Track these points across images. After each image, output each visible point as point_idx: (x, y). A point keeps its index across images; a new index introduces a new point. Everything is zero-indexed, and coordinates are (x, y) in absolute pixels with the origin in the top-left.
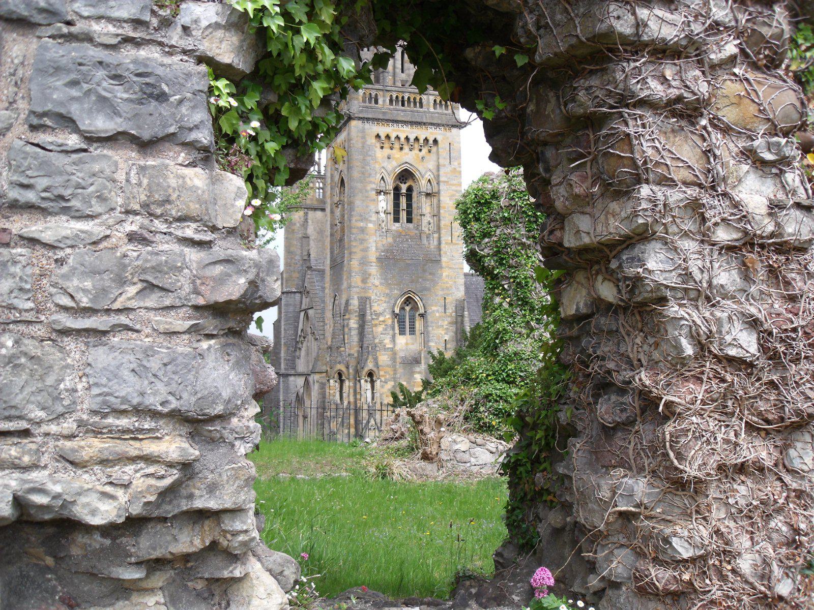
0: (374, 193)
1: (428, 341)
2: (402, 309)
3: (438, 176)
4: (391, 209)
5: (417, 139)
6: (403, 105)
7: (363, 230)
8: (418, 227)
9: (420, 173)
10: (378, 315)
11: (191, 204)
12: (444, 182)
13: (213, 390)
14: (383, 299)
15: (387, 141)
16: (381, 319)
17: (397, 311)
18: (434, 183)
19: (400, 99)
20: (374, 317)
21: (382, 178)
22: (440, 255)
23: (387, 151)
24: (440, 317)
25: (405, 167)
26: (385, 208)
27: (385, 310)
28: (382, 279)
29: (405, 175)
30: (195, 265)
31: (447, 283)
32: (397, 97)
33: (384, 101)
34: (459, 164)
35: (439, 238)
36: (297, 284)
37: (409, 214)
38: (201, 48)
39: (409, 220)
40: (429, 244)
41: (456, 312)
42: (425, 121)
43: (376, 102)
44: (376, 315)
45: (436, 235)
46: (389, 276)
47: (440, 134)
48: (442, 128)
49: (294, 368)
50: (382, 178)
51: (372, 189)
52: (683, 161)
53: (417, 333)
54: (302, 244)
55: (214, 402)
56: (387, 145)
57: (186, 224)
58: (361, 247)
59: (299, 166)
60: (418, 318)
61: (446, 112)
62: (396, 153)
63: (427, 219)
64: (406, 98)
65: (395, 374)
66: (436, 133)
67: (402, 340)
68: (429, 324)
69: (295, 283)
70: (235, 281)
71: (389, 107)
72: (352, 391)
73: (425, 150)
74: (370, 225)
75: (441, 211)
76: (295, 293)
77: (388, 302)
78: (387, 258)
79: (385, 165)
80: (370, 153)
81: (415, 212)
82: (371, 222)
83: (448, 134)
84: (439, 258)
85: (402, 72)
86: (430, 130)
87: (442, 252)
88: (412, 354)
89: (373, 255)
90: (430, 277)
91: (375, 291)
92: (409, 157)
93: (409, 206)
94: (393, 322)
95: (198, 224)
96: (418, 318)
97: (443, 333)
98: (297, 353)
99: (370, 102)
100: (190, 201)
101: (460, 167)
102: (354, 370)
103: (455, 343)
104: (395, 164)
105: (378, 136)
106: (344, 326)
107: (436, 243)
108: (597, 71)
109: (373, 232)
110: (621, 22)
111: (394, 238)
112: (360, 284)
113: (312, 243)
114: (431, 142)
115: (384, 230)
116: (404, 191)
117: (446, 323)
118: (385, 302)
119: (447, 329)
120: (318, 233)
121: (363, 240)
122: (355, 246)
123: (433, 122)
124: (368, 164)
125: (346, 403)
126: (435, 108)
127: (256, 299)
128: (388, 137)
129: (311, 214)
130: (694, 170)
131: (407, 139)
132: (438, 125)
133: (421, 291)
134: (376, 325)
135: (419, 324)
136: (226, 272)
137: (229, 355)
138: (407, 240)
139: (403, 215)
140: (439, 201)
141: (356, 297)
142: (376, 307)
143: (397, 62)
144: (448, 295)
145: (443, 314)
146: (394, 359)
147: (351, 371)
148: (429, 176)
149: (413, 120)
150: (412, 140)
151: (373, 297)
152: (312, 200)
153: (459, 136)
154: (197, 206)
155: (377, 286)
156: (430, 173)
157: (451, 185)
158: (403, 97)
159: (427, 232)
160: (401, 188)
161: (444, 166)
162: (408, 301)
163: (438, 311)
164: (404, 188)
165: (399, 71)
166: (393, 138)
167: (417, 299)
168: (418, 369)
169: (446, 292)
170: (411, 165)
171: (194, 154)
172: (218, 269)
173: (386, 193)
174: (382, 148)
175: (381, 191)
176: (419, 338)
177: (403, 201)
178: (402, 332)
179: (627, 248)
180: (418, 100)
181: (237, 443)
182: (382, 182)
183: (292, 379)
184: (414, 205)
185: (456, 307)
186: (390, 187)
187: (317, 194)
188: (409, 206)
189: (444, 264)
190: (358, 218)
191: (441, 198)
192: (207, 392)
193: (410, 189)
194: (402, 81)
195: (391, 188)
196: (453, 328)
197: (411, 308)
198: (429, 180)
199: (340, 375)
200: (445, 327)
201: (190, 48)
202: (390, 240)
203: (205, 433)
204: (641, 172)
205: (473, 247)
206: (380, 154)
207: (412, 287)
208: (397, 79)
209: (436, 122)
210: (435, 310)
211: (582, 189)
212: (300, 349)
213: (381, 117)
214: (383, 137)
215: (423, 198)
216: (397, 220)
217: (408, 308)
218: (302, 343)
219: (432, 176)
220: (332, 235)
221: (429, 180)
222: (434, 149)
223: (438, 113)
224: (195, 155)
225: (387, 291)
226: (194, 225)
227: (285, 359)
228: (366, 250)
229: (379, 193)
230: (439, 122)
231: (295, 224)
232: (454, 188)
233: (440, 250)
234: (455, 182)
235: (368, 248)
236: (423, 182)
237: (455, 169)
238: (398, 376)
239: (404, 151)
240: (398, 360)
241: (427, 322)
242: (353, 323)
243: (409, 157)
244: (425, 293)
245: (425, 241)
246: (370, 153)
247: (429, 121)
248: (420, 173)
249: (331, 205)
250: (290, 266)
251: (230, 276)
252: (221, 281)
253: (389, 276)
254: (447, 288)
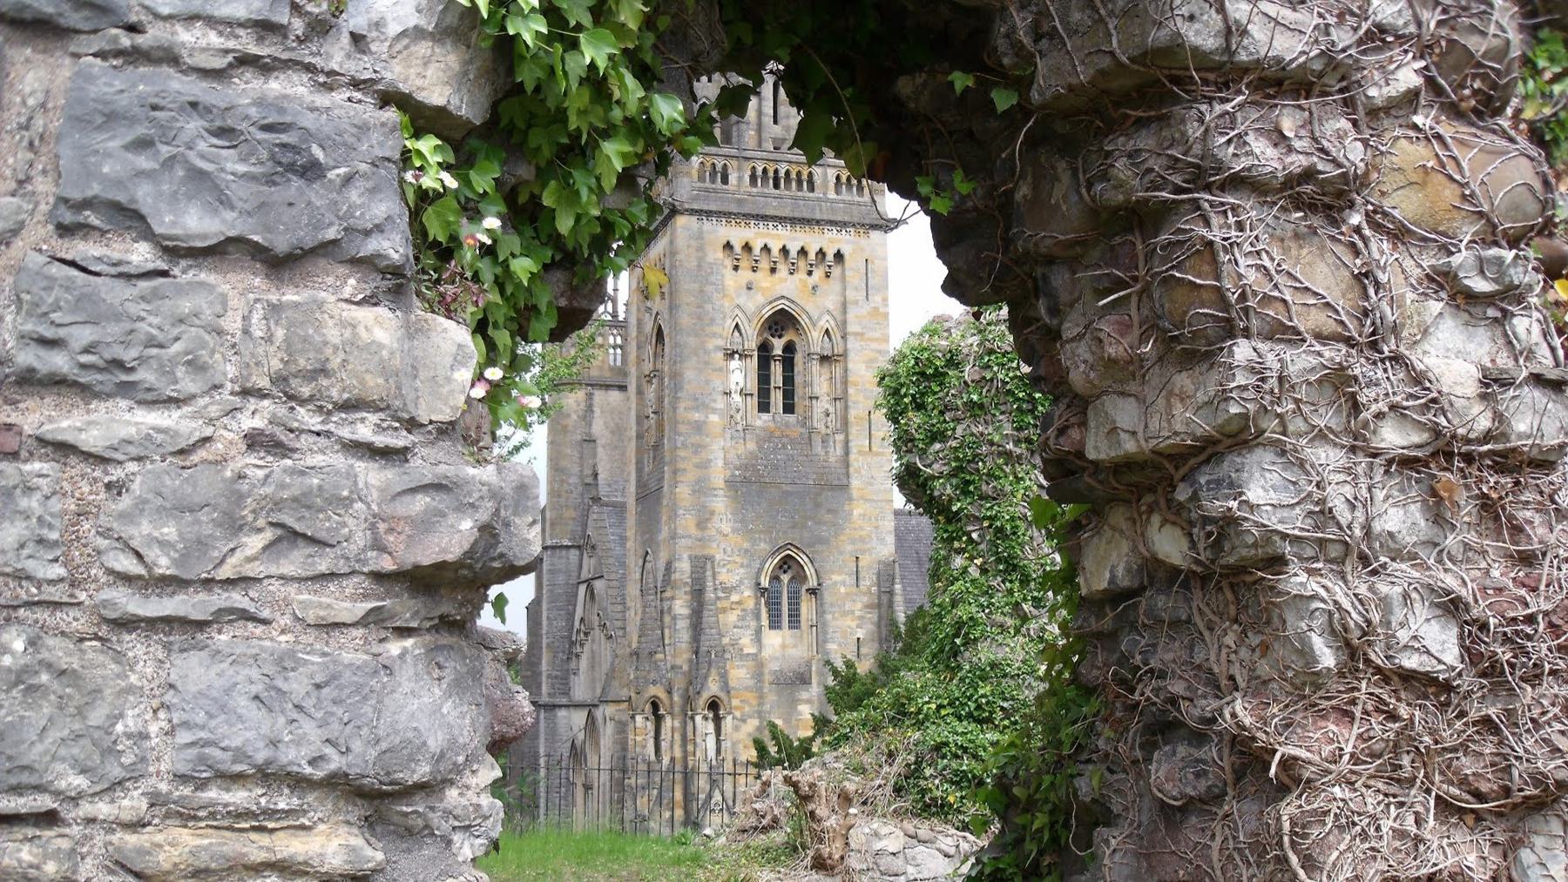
0: (720, 355)
1: (825, 641)
2: (775, 578)
3: (845, 322)
4: (753, 386)
5: (803, 252)
6: (776, 186)
7: (699, 427)
8: (805, 421)
9: (810, 318)
10: (728, 590)
11: (368, 377)
12: (856, 334)
13: (410, 735)
14: (738, 559)
15: (745, 255)
16: (735, 597)
17: (765, 583)
18: (836, 336)
19: (771, 174)
20: (721, 594)
21: (737, 326)
22: (848, 477)
23: (745, 275)
24: (847, 594)
25: (780, 304)
26: (742, 384)
27: (741, 582)
28: (736, 522)
29: (781, 321)
30: (375, 494)
31: (861, 528)
32: (765, 171)
33: (740, 178)
34: (885, 300)
35: (847, 442)
36: (572, 531)
37: (789, 395)
38: (388, 75)
39: (789, 408)
40: (827, 453)
41: (879, 586)
42: (818, 216)
43: (725, 180)
44: (725, 590)
45: (840, 437)
46: (751, 515)
47: (848, 242)
48: (852, 230)
49: (566, 693)
50: (737, 326)
51: (718, 348)
52: (1316, 294)
53: (804, 624)
54: (581, 453)
55: (411, 759)
56: (744, 264)
57: (359, 415)
58: (696, 460)
59: (575, 304)
60: (804, 596)
61: (860, 199)
62: (762, 278)
63: (823, 405)
64: (782, 173)
65: (761, 704)
66: (840, 241)
67: (774, 640)
68: (827, 607)
69: (569, 528)
70: (452, 526)
71: (749, 189)
72: (677, 737)
73: (818, 273)
74: (714, 418)
75: (851, 391)
76: (568, 547)
77: (749, 566)
78: (746, 481)
79: (741, 301)
80: (713, 279)
81: (799, 391)
82: (714, 411)
83: (863, 241)
84: (845, 482)
85: (775, 122)
86: (828, 235)
87: (851, 470)
88: (794, 666)
89: (718, 476)
90: (829, 517)
91: (723, 546)
92: (788, 287)
93: (789, 380)
94: (758, 603)
95: (382, 415)
96: (804, 596)
97: (854, 624)
98: (573, 665)
99: (713, 181)
100: (367, 371)
101: (887, 305)
102: (682, 696)
103: (876, 645)
104: (760, 299)
105: (728, 246)
106: (662, 612)
107: (839, 451)
108: (1149, 120)
109: (718, 430)
110: (1197, 26)
111: (760, 442)
112: (693, 531)
113: (600, 450)
114: (830, 257)
115: (740, 427)
116: (778, 351)
117: (859, 605)
118: (742, 566)
119: (861, 618)
120: (612, 432)
121: (699, 446)
122: (684, 459)
123: (832, 218)
124: (710, 300)
125: (666, 761)
126: (838, 192)
127: (494, 559)
128: (747, 248)
129: (599, 395)
130: (1337, 312)
131: (784, 251)
132: (841, 225)
133: (811, 545)
134: (724, 610)
135: (807, 608)
136: (435, 508)
137: (440, 667)
138: (784, 446)
139: (777, 398)
140: (846, 371)
141: (685, 556)
142: (727, 576)
143: (764, 103)
144: (864, 552)
145: (854, 589)
146: (758, 675)
147: (676, 698)
148: (825, 322)
149: (797, 215)
150: (793, 253)
151: (718, 557)
152: (601, 368)
153: (884, 245)
154: (380, 381)
155: (726, 535)
156: (828, 317)
157: (869, 339)
158: (776, 171)
159: (823, 430)
160: (772, 348)
161: (856, 303)
162: (787, 563)
163: (844, 583)
164: (778, 346)
165: (768, 120)
166: (757, 250)
167: (803, 559)
168: (804, 695)
169: (859, 545)
170: (793, 302)
171: (374, 280)
172: (421, 502)
173: (743, 356)
174: (736, 268)
175: (734, 352)
176: (807, 635)
177: (777, 370)
178: (775, 624)
179: (1207, 461)
180: (805, 177)
181: (457, 838)
182: (736, 334)
183: (562, 713)
184: (798, 379)
185: (879, 575)
186: (752, 344)
187: (612, 357)
188: (789, 380)
189: (855, 493)
190: (690, 403)
191: (850, 366)
192: (397, 741)
193: (789, 348)
194: (774, 140)
195: (754, 346)
196: (874, 616)
197: (793, 578)
198: (827, 330)
199: (655, 706)
200: (858, 613)
201: (367, 75)
202: (751, 446)
203: (396, 819)
204: (1234, 314)
205: (912, 460)
206: (733, 281)
207: (794, 537)
208: (765, 135)
209: (840, 219)
210: (838, 582)
211: (1121, 348)
212: (578, 656)
213: (733, 208)
214: (738, 249)
215: (815, 366)
216: (764, 407)
217: (785, 578)
218: (582, 645)
219: (832, 323)
220: (639, 436)
221: (827, 330)
222: (836, 271)
223: (844, 202)
224: (376, 282)
225: (746, 545)
226: (373, 418)
227: (549, 676)
228: (705, 465)
229: (730, 355)
230: (846, 219)
231: (569, 415)
232: (874, 346)
233: (847, 466)
234: (877, 335)
235: (710, 461)
236: (815, 335)
237: (876, 309)
238: (767, 707)
239: (777, 275)
240: (768, 678)
241: (822, 605)
242: (681, 607)
243: (788, 287)
244: (819, 547)
245: (818, 448)
246: (713, 279)
247: (825, 217)
248: (810, 318)
249: (638, 378)
250: (559, 496)
251: (444, 515)
252: (425, 524)
253: (751, 515)
254: (862, 539)
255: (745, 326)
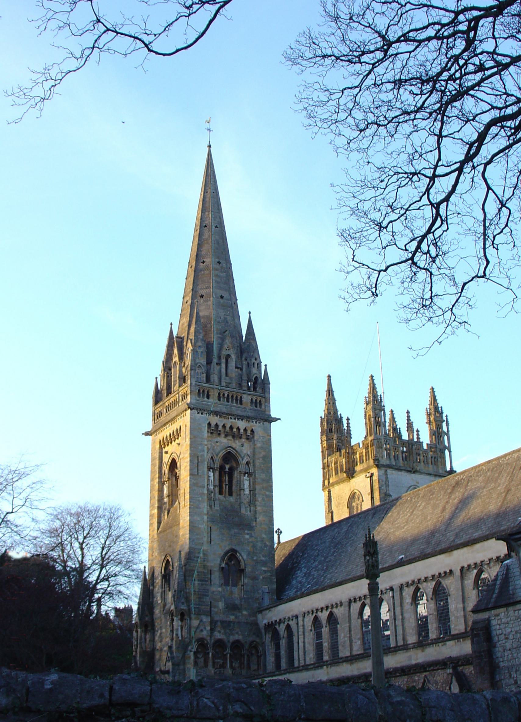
6: (228, 401)
17: (223, 565)
18: (251, 466)
99: (203, 397)
105: (209, 424)
139: (226, 488)
164: (227, 467)
184: (234, 481)
186: (217, 466)
193: (231, 469)
216: (221, 493)
255: (215, 457)
